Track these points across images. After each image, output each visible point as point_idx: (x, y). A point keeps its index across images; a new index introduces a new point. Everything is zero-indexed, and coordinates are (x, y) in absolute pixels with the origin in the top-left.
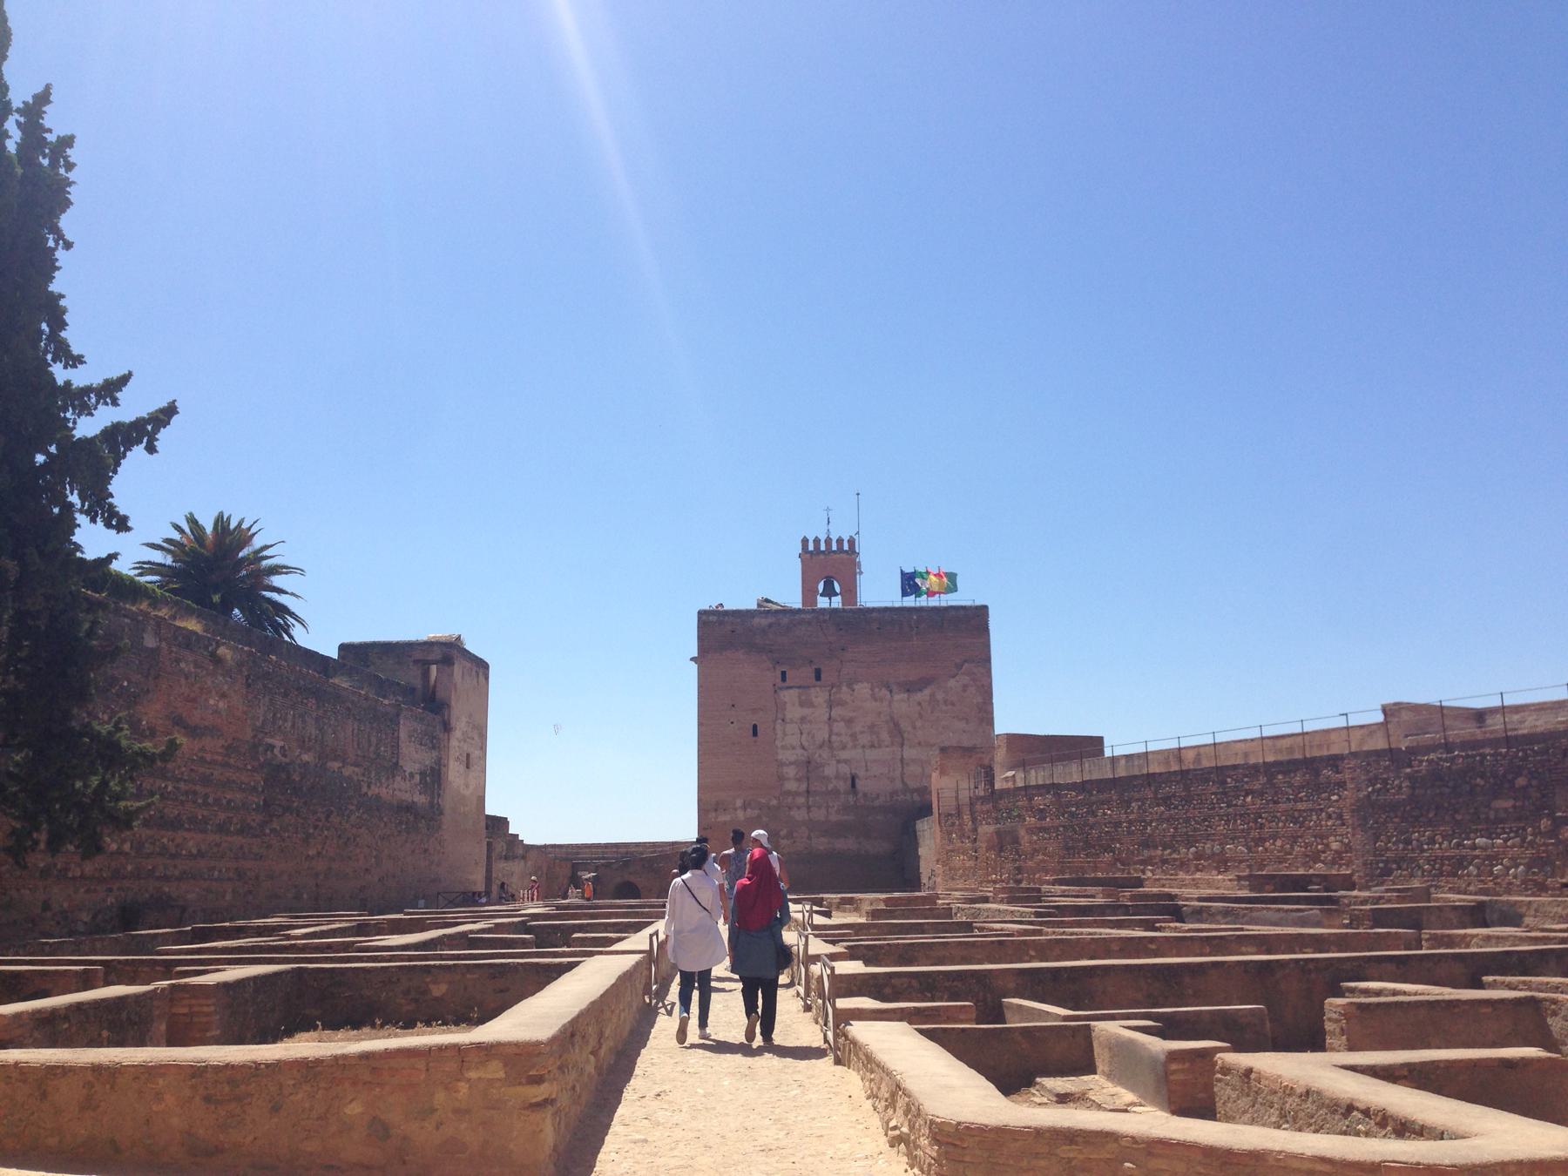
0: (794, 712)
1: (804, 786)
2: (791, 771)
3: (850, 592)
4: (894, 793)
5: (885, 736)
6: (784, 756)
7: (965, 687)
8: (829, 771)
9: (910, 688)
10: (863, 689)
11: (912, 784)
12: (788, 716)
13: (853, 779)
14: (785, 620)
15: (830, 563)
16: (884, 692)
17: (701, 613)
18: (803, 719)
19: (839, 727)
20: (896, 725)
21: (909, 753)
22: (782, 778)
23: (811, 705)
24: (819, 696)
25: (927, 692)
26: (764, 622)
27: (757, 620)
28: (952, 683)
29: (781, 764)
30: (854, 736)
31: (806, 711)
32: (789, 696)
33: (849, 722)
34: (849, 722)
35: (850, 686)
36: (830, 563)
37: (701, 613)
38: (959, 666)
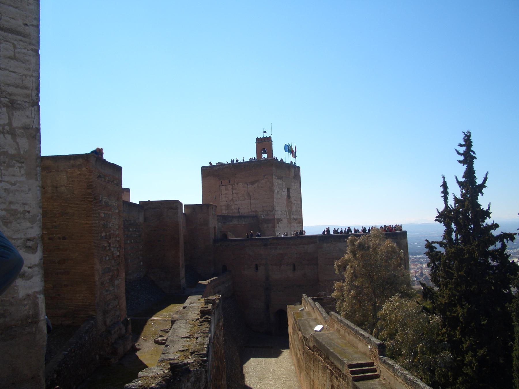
0: (224, 192)
1: (227, 212)
2: (224, 208)
3: (270, 152)
4: (249, 212)
5: (246, 197)
6: (222, 204)
7: (266, 182)
8: (233, 207)
9: (252, 183)
10: (240, 185)
11: (253, 210)
12: (223, 193)
13: (239, 209)
14: (222, 167)
15: (264, 144)
16: (246, 185)
17: (202, 167)
18: (226, 194)
19: (235, 195)
20: (249, 194)
21: (252, 201)
22: (221, 210)
23: (228, 190)
24: (230, 187)
25: (257, 184)
26: (217, 168)
27: (215, 168)
28: (263, 181)
29: (221, 206)
30: (239, 198)
31: (227, 192)
32: (223, 188)
33: (237, 194)
34: (237, 194)
35: (237, 184)
36: (264, 144)
37: (202, 167)
38: (264, 176)
